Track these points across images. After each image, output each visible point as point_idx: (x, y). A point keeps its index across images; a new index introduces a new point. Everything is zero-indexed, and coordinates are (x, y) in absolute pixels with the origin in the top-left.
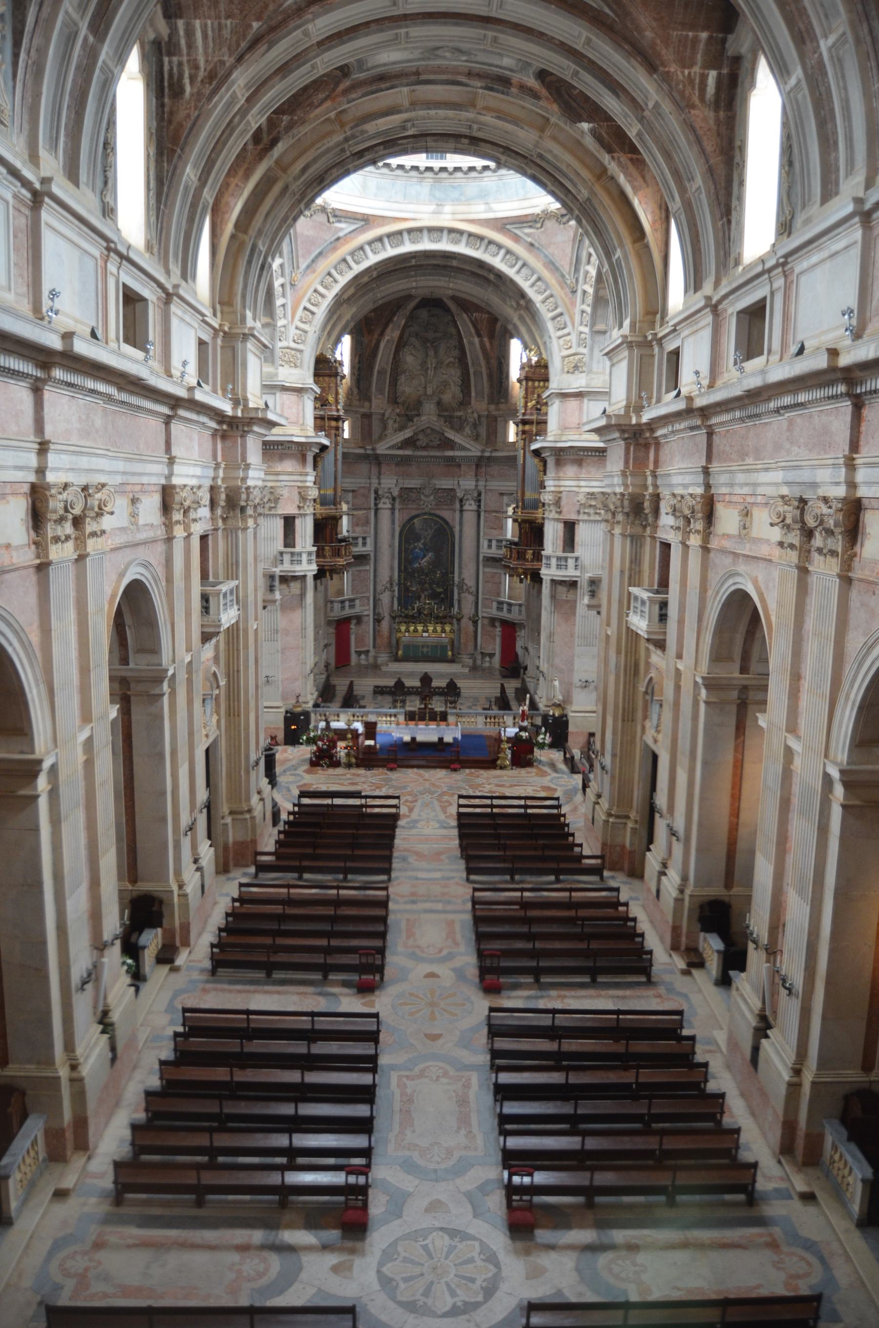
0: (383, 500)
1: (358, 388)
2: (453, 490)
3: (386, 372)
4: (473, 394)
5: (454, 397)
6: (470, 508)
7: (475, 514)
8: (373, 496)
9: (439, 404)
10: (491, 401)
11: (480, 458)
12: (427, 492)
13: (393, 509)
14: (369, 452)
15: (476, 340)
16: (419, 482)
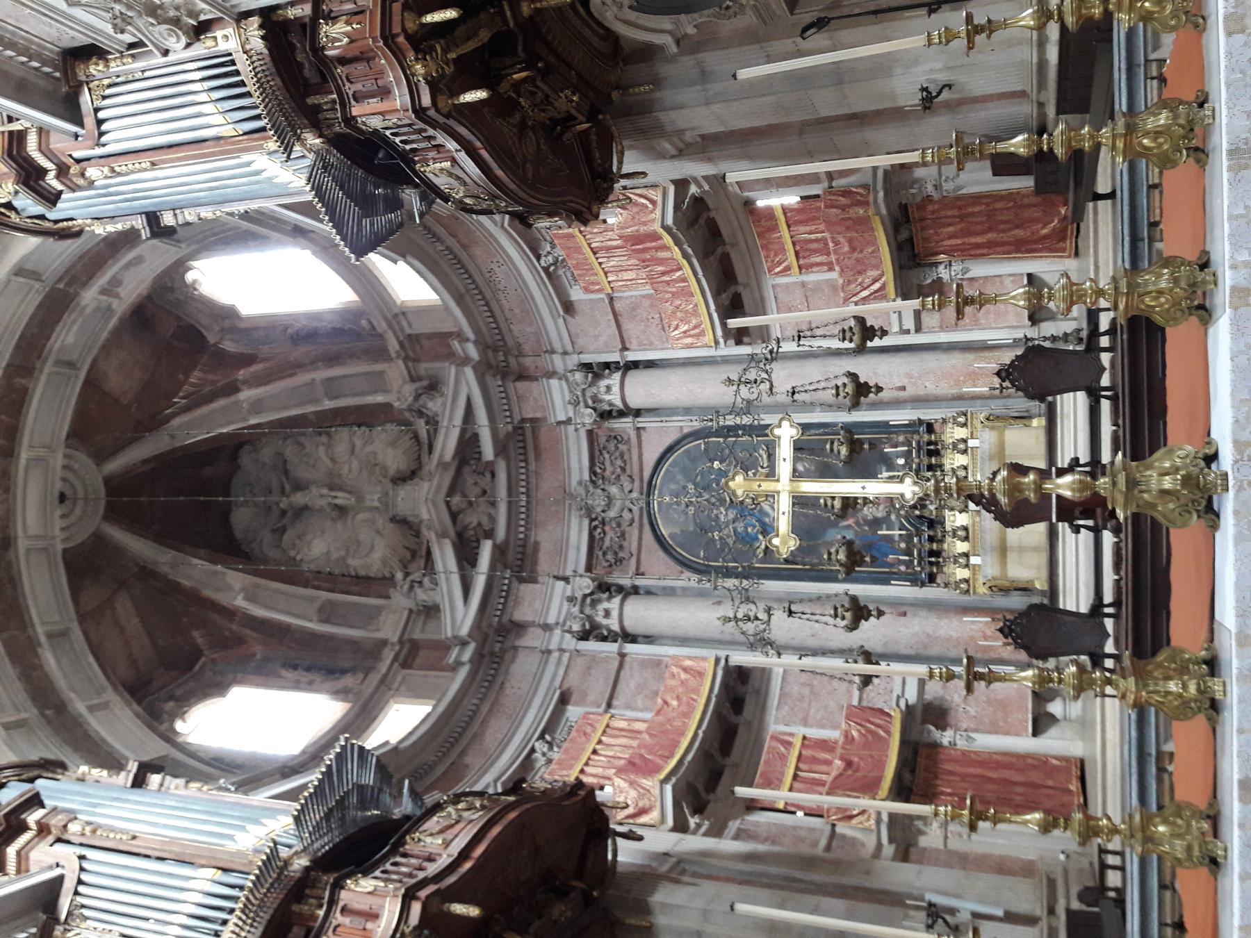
0: (600, 619)
1: (344, 672)
2: (590, 433)
3: (332, 603)
4: (380, 399)
5: (393, 444)
6: (616, 389)
7: (634, 378)
8: (592, 646)
9: (402, 479)
10: (380, 354)
11: (485, 369)
12: (599, 502)
13: (635, 590)
14: (467, 655)
15: (246, 395)
16: (575, 522)
